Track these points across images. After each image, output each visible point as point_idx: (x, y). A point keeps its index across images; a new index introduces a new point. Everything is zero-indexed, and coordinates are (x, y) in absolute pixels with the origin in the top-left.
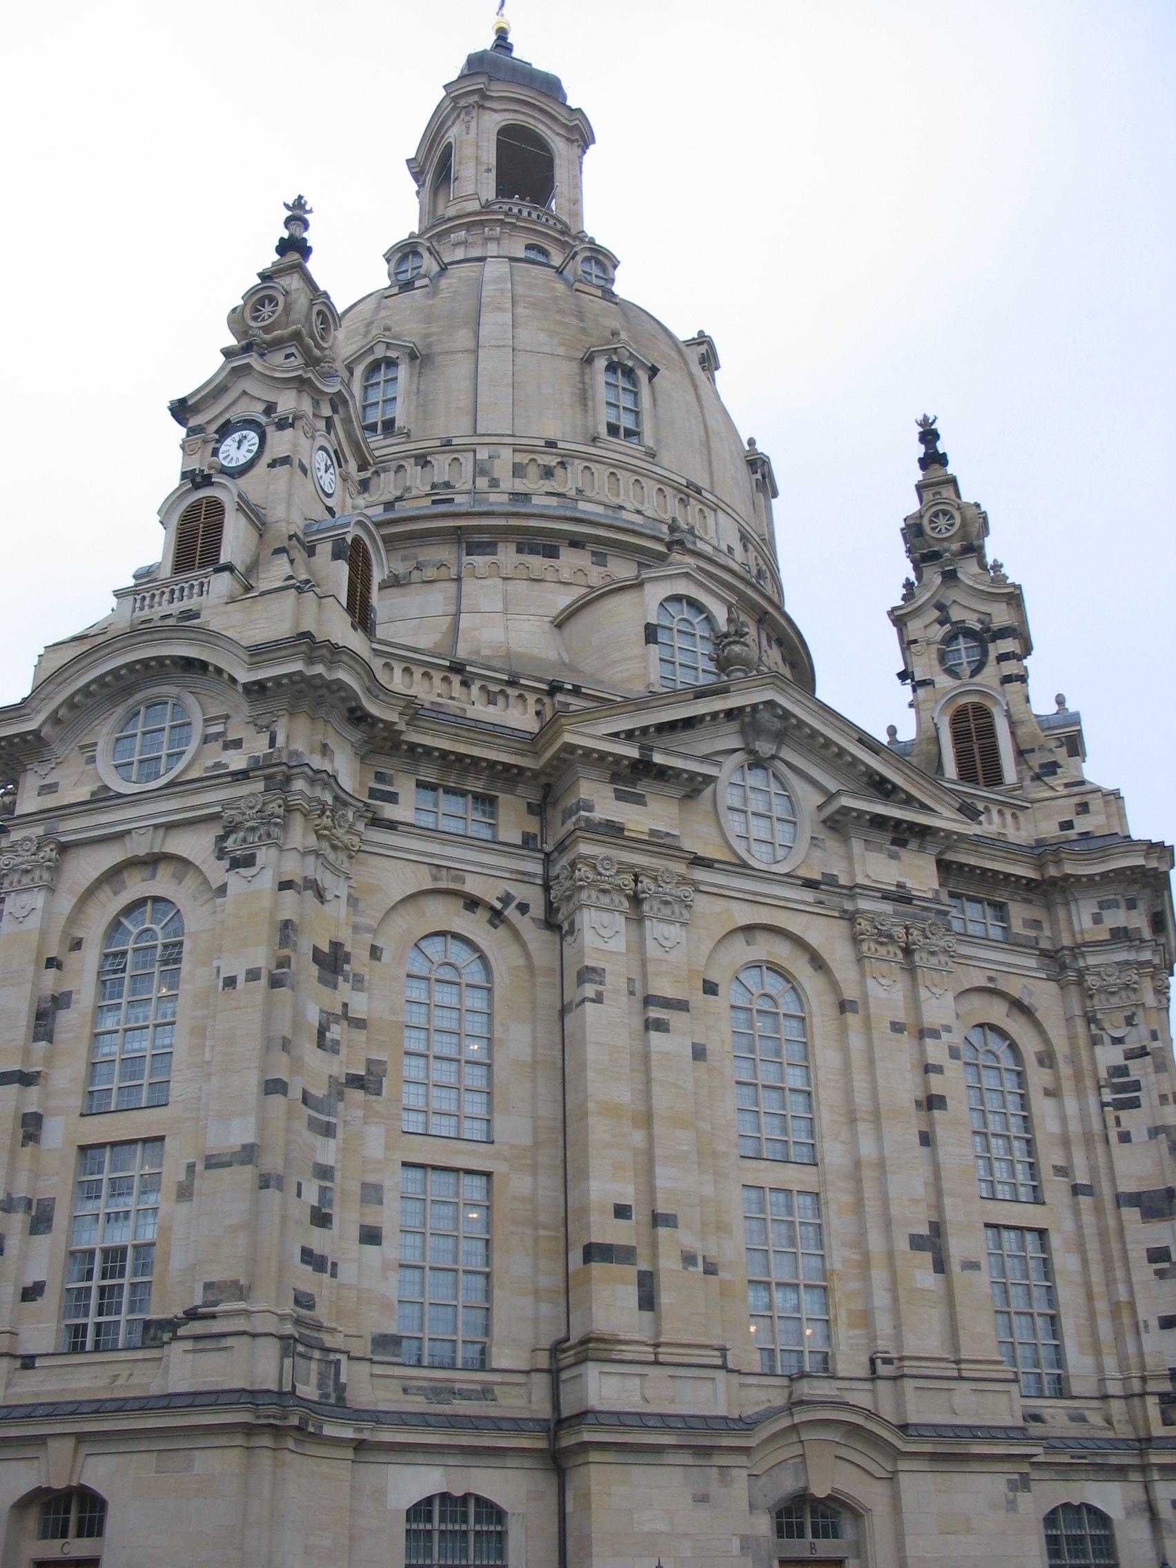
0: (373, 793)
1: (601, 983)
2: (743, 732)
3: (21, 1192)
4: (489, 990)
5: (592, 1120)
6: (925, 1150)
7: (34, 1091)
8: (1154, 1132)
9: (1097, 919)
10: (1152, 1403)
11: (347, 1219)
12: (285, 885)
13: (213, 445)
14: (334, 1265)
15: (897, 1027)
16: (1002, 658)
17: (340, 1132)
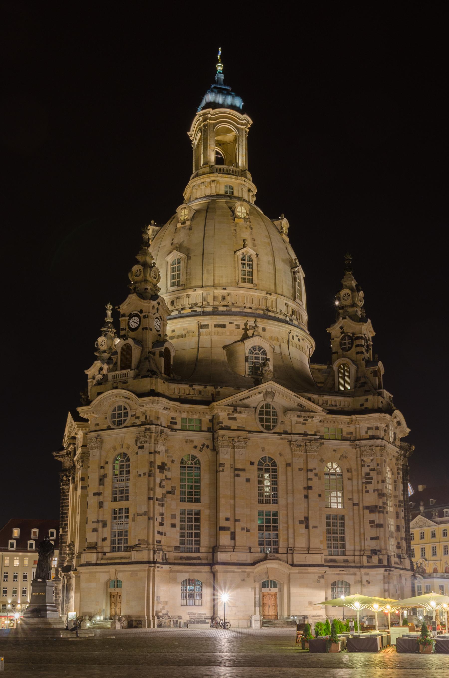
0: (171, 423)
1: (224, 467)
2: (264, 396)
3: (100, 519)
4: (199, 468)
5: (220, 499)
6: (306, 500)
7: (101, 496)
8: (374, 491)
9: (367, 432)
10: (365, 558)
11: (167, 522)
12: (150, 453)
13: (128, 320)
14: (165, 533)
15: (300, 470)
16: (357, 346)
17: (165, 505)
